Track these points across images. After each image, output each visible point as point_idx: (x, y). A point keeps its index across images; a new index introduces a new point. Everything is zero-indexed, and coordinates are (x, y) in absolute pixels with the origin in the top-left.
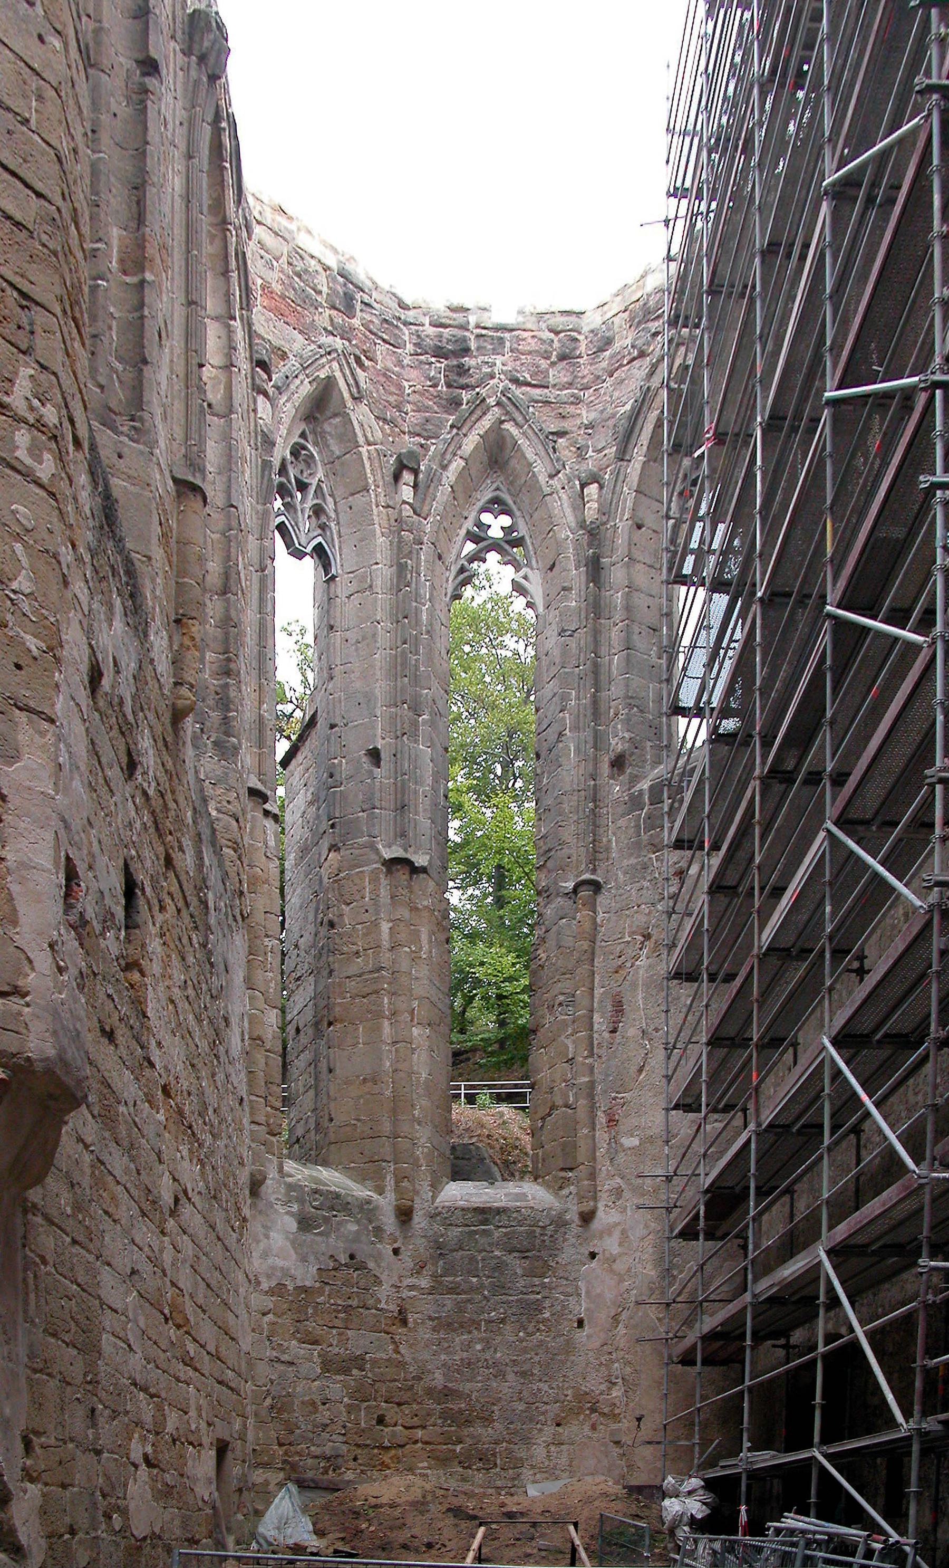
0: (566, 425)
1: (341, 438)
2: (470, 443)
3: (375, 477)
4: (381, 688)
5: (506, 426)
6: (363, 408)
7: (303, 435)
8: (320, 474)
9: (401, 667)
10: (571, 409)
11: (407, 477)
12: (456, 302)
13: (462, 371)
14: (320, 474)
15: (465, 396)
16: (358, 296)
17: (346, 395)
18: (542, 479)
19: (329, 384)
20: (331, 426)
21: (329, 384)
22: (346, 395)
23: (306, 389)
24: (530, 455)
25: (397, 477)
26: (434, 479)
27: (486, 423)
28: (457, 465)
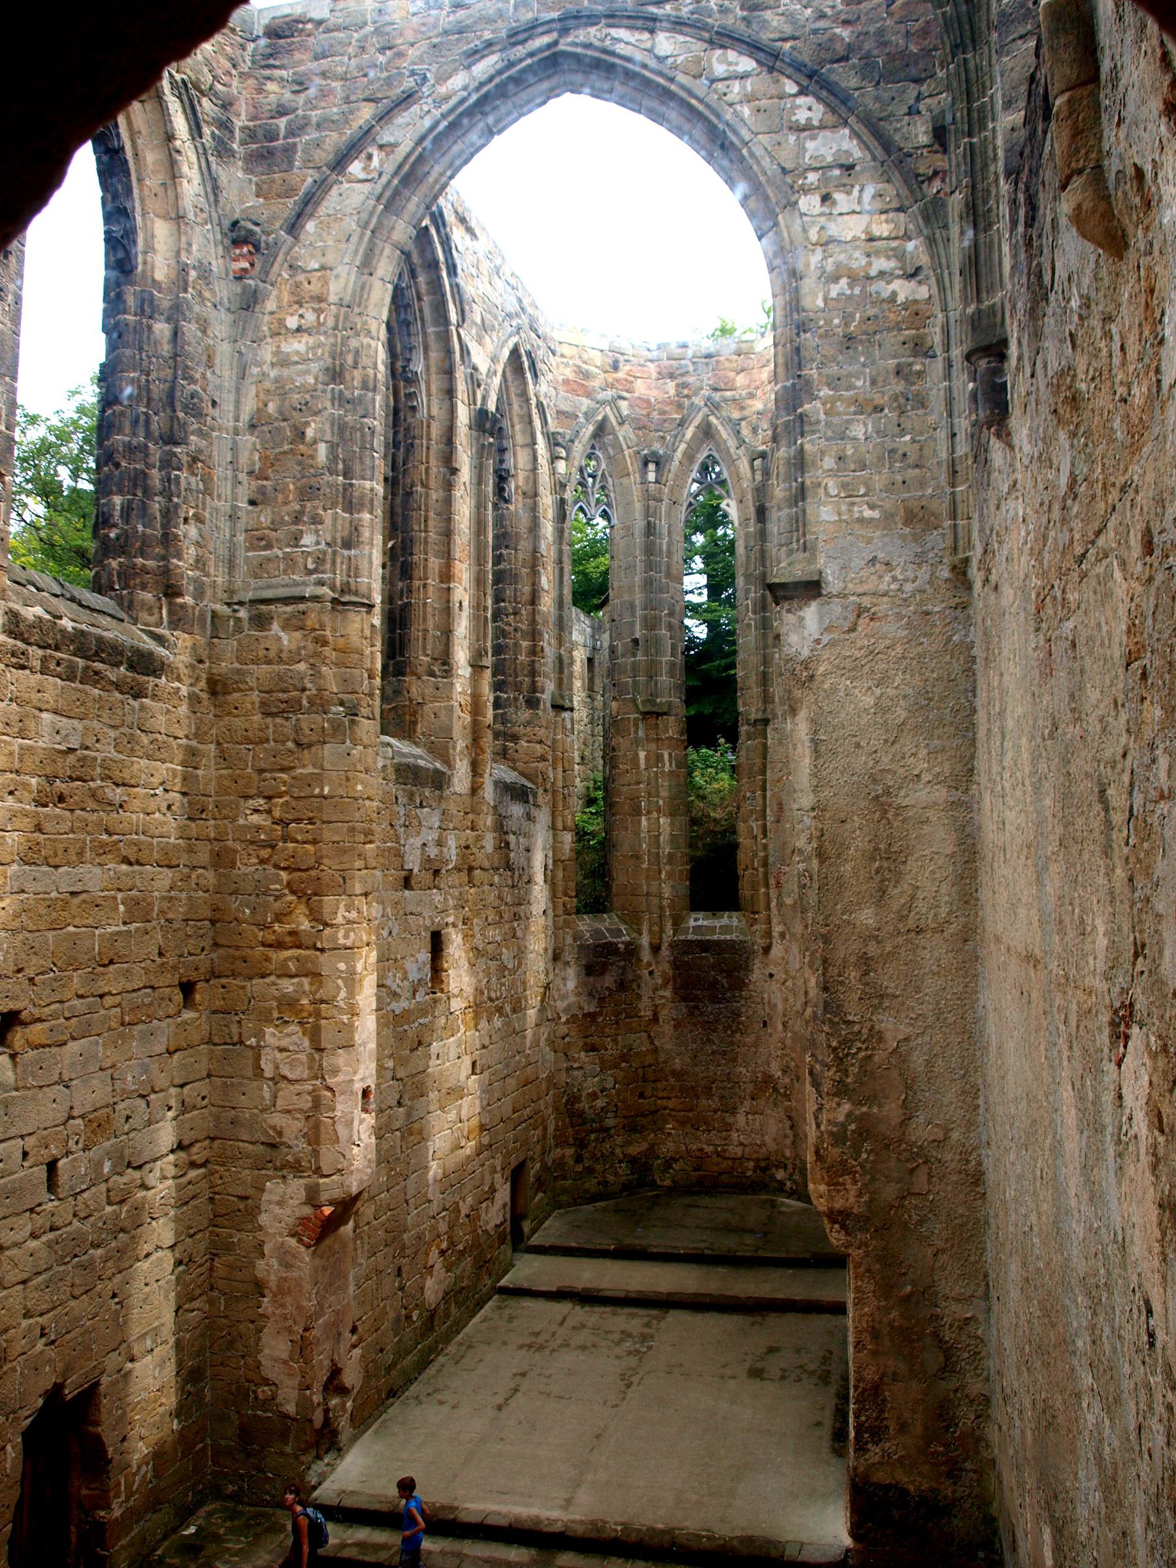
0: (746, 413)
1: (613, 447)
2: (689, 433)
3: (632, 465)
4: (638, 598)
5: (712, 419)
6: (626, 426)
7: (593, 447)
8: (603, 466)
9: (648, 584)
10: (749, 402)
11: (652, 467)
12: (682, 340)
13: (684, 385)
14: (603, 466)
15: (686, 402)
16: (621, 359)
17: (614, 423)
18: (732, 450)
19: (605, 418)
20: (608, 439)
21: (605, 418)
22: (614, 423)
23: (591, 428)
24: (724, 435)
25: (646, 464)
26: (669, 458)
27: (696, 423)
28: (683, 446)
